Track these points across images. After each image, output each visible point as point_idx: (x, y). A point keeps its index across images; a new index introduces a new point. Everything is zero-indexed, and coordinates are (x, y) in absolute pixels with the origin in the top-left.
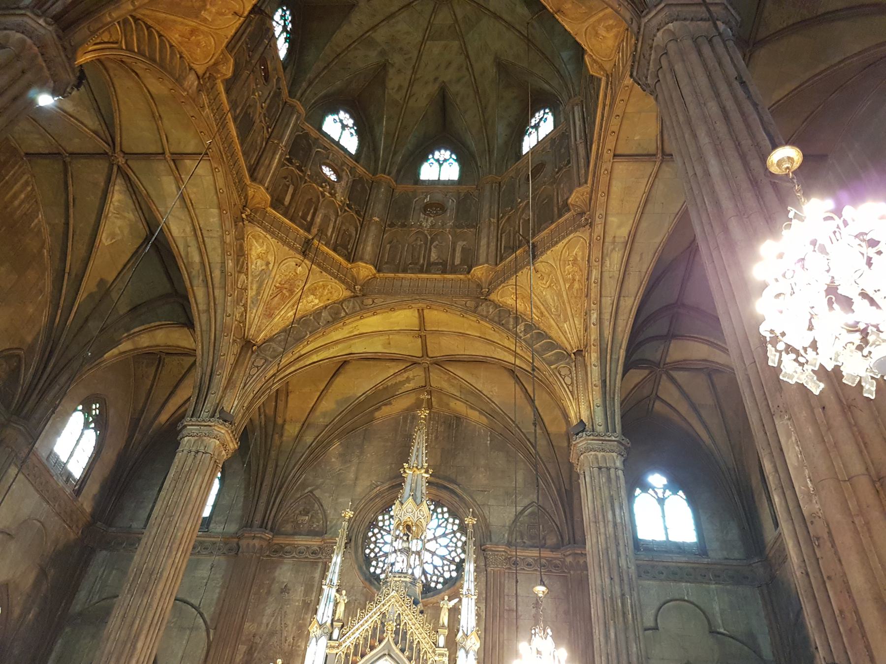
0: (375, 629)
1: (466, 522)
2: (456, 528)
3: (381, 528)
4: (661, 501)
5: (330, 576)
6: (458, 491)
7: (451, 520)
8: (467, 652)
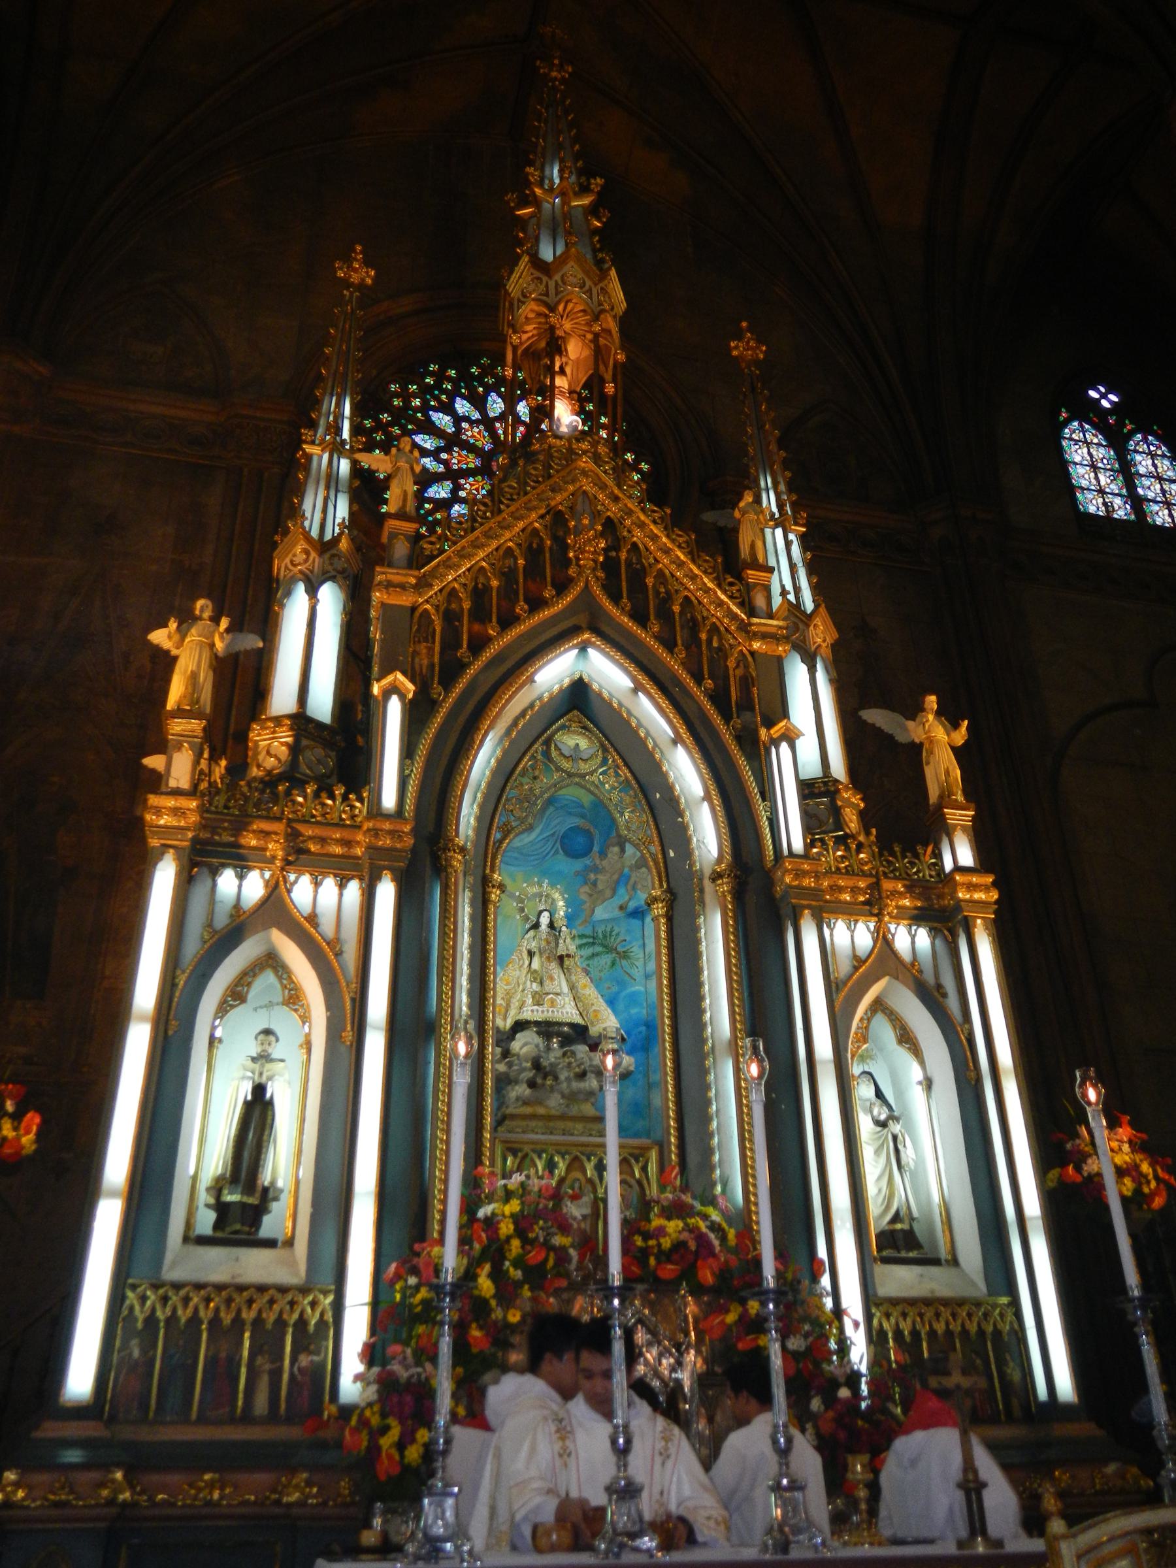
0: (534, 553)
1: (735, 353)
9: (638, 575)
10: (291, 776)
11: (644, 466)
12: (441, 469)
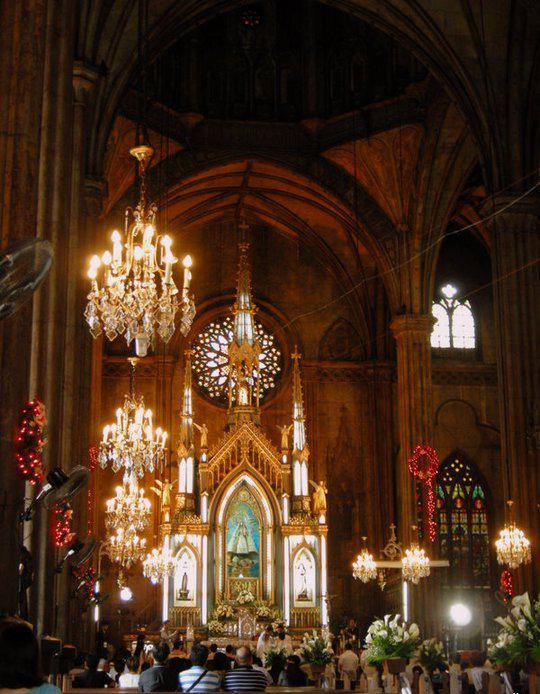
0: (233, 453)
2: (271, 343)
3: (202, 346)
4: (450, 311)
5: (185, 410)
6: (272, 309)
7: (266, 336)
8: (301, 463)
9: (257, 455)
10: (183, 510)
11: (279, 353)
12: (215, 365)
